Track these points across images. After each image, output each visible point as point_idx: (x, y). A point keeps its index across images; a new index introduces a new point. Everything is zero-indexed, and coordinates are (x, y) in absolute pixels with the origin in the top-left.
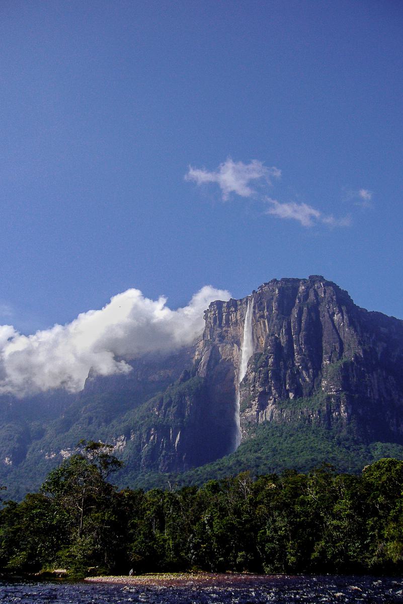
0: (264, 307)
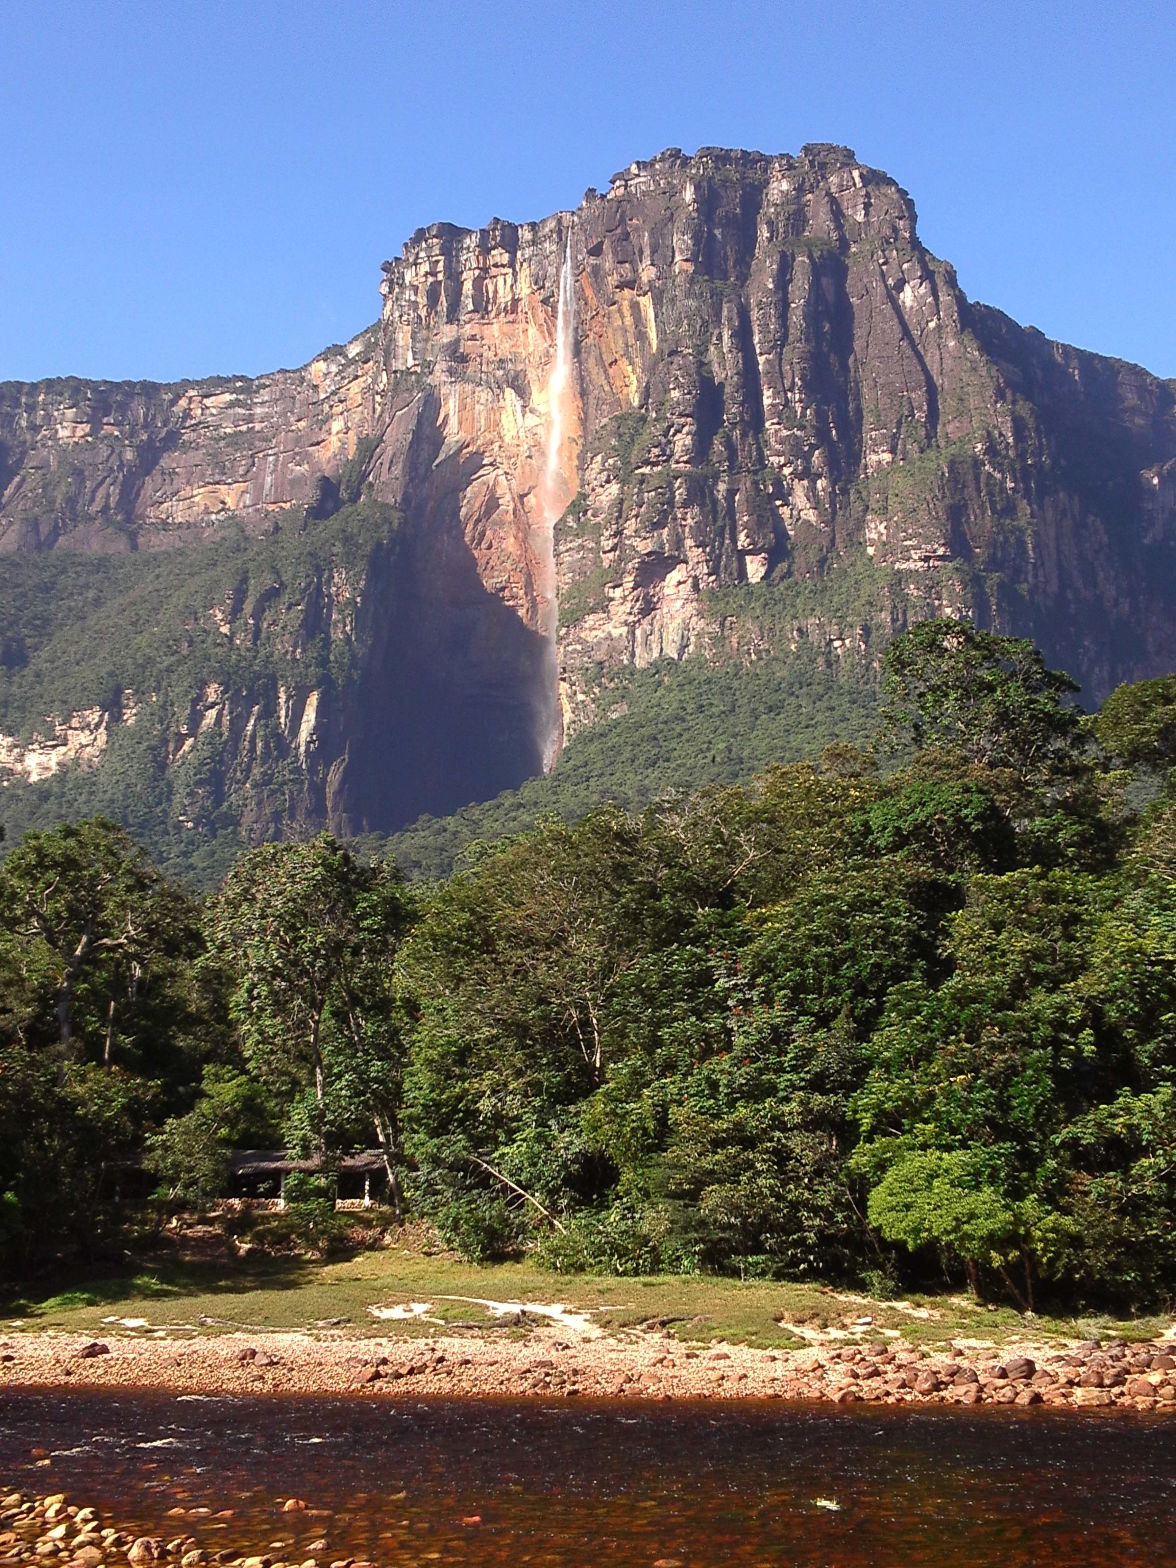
0: (641, 252)
